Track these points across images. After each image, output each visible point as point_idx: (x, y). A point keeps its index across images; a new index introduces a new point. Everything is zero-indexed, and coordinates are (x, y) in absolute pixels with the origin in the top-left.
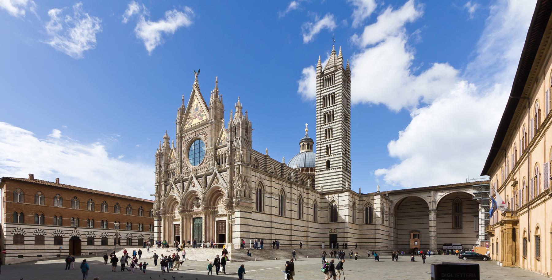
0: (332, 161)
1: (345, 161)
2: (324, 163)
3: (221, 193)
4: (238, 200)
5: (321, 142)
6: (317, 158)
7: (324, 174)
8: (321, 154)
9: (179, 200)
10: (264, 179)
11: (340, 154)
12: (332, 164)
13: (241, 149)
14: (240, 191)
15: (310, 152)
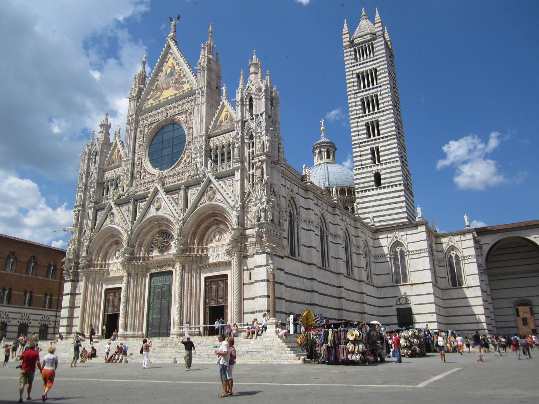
0: (385, 174)
1: (405, 173)
2: (370, 177)
3: (217, 220)
4: (260, 230)
5: (361, 143)
6: (356, 169)
7: (371, 196)
8: (363, 163)
9: (125, 237)
10: (297, 193)
11: (397, 161)
12: (385, 178)
13: (264, 132)
14: (265, 211)
15: (333, 163)
